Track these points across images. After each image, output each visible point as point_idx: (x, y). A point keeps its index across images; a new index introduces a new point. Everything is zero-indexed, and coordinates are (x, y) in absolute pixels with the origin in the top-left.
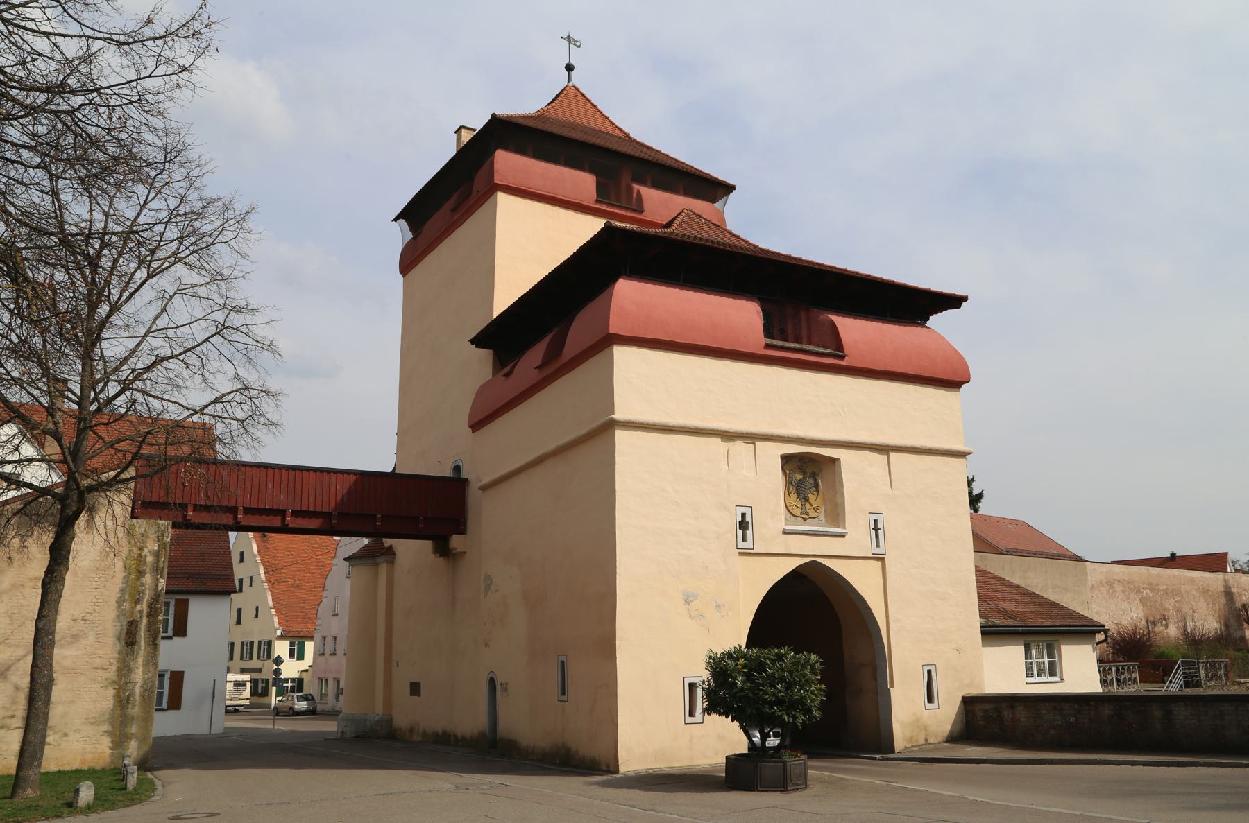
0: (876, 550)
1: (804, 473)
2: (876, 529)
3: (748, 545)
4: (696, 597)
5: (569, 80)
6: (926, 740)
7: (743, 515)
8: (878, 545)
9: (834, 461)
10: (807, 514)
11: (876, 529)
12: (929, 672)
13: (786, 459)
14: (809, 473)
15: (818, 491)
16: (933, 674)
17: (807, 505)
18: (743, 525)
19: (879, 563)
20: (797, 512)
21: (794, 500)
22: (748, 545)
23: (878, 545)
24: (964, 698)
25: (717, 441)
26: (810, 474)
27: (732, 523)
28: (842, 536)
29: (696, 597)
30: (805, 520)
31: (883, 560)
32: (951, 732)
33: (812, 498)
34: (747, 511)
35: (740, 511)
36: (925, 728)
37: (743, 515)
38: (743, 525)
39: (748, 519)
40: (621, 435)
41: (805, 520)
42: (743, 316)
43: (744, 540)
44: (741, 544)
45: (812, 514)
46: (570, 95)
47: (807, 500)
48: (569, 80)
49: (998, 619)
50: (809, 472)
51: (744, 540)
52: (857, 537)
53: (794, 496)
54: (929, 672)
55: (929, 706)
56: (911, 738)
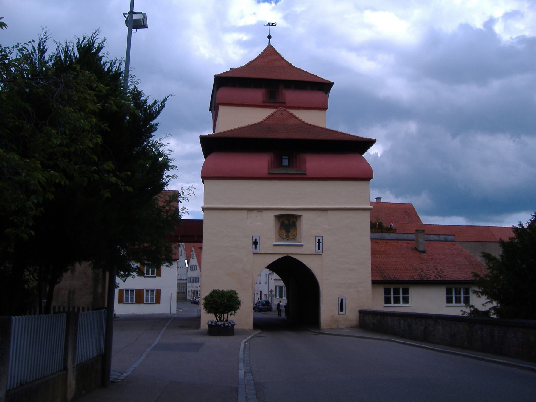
0: (318, 251)
2: (319, 242)
3: (257, 250)
7: (256, 240)
8: (319, 249)
9: (300, 216)
11: (319, 242)
12: (342, 300)
13: (278, 217)
16: (344, 301)
17: (290, 234)
18: (256, 243)
20: (284, 237)
21: (284, 233)
23: (319, 249)
25: (246, 212)
27: (250, 242)
30: (288, 240)
33: (292, 231)
34: (257, 238)
35: (254, 238)
37: (256, 240)
38: (256, 243)
42: (261, 162)
44: (254, 250)
54: (342, 300)
55: (341, 313)
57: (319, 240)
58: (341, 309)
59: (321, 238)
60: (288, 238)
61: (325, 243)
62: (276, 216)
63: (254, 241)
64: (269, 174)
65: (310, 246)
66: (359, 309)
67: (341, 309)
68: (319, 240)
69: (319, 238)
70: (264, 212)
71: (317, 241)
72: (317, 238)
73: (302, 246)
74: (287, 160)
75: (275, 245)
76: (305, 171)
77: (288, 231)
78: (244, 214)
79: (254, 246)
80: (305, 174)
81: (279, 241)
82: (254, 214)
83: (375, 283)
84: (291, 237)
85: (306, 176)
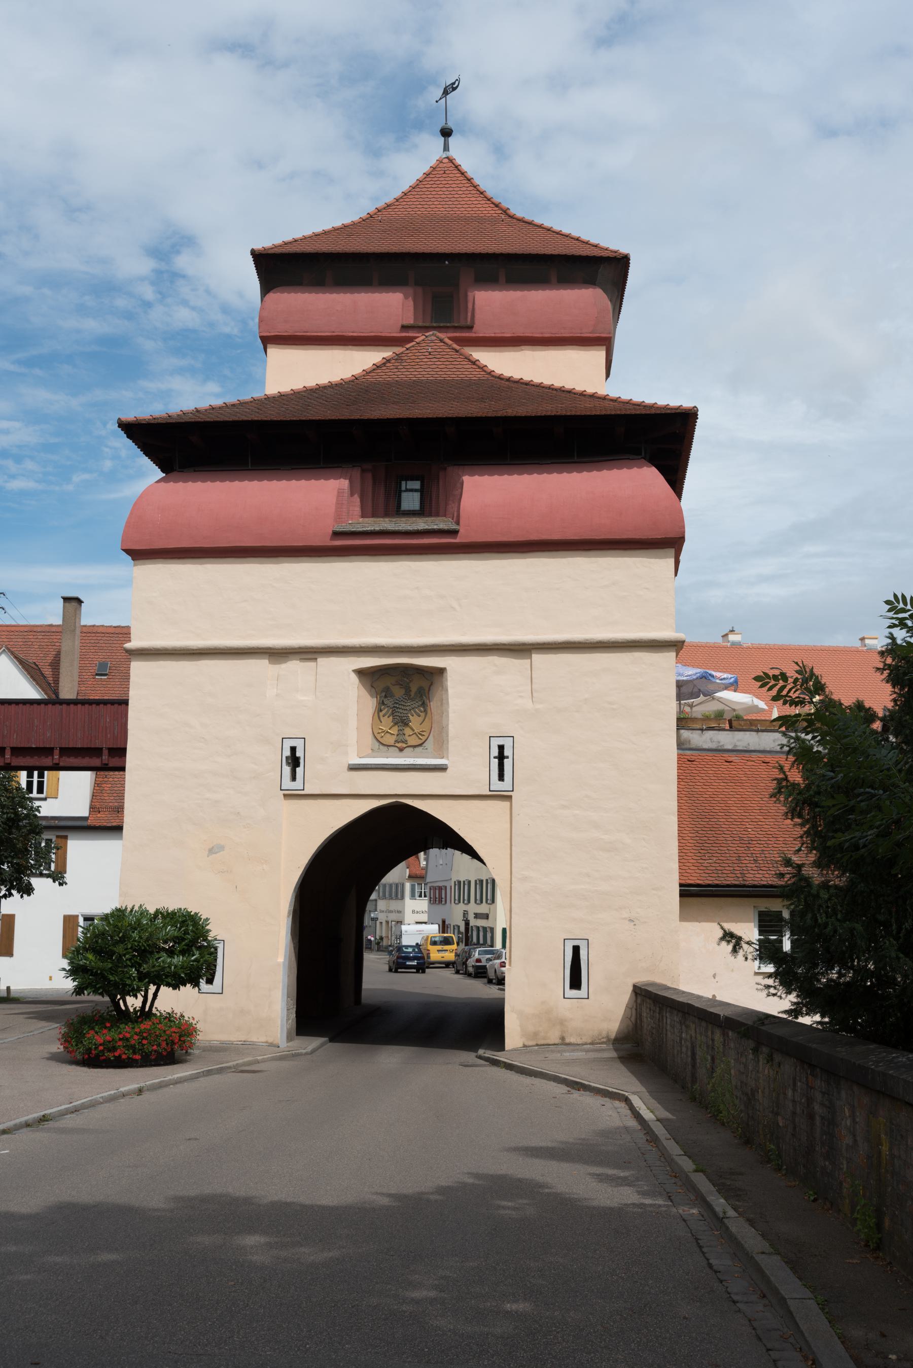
0: (497, 785)
1: (408, 690)
2: (501, 757)
3: (298, 784)
4: (221, 848)
5: (446, 148)
6: (563, 1038)
7: (293, 749)
8: (501, 777)
9: (441, 671)
10: (405, 742)
11: (501, 757)
12: (576, 950)
14: (404, 688)
15: (425, 711)
17: (408, 731)
18: (294, 761)
19: (507, 804)
20: (390, 740)
22: (298, 784)
23: (501, 777)
24: (635, 987)
26: (404, 688)
27: (275, 758)
28: (442, 769)
29: (221, 848)
31: (509, 798)
32: (618, 1032)
33: (415, 721)
34: (299, 744)
35: (288, 744)
36: (562, 1022)
37: (293, 749)
38: (294, 761)
39: (299, 753)
40: (137, 668)
41: (401, 750)
42: (319, 498)
43: (294, 778)
44: (288, 784)
45: (413, 741)
46: (447, 172)
47: (405, 723)
48: (446, 148)
49: (683, 882)
50: (414, 689)
51: (294, 778)
52: (468, 767)
53: (387, 721)
54: (576, 950)
55: (575, 993)
56: (536, 1034)
57: (501, 748)
58: (576, 983)
59: (507, 743)
60: (401, 746)
61: (521, 761)
62: (360, 673)
63: (287, 753)
64: (336, 534)
65: (468, 767)
66: (642, 978)
67: (576, 983)
68: (501, 748)
69: (501, 742)
70: (323, 662)
71: (495, 752)
72: (496, 743)
73: (442, 769)
74: (417, 496)
75: (353, 768)
76: (458, 523)
77: (403, 722)
78: (261, 664)
79: (287, 770)
80: (454, 533)
81: (374, 752)
82: (294, 666)
83: (691, 893)
84: (413, 741)
85: (457, 540)
